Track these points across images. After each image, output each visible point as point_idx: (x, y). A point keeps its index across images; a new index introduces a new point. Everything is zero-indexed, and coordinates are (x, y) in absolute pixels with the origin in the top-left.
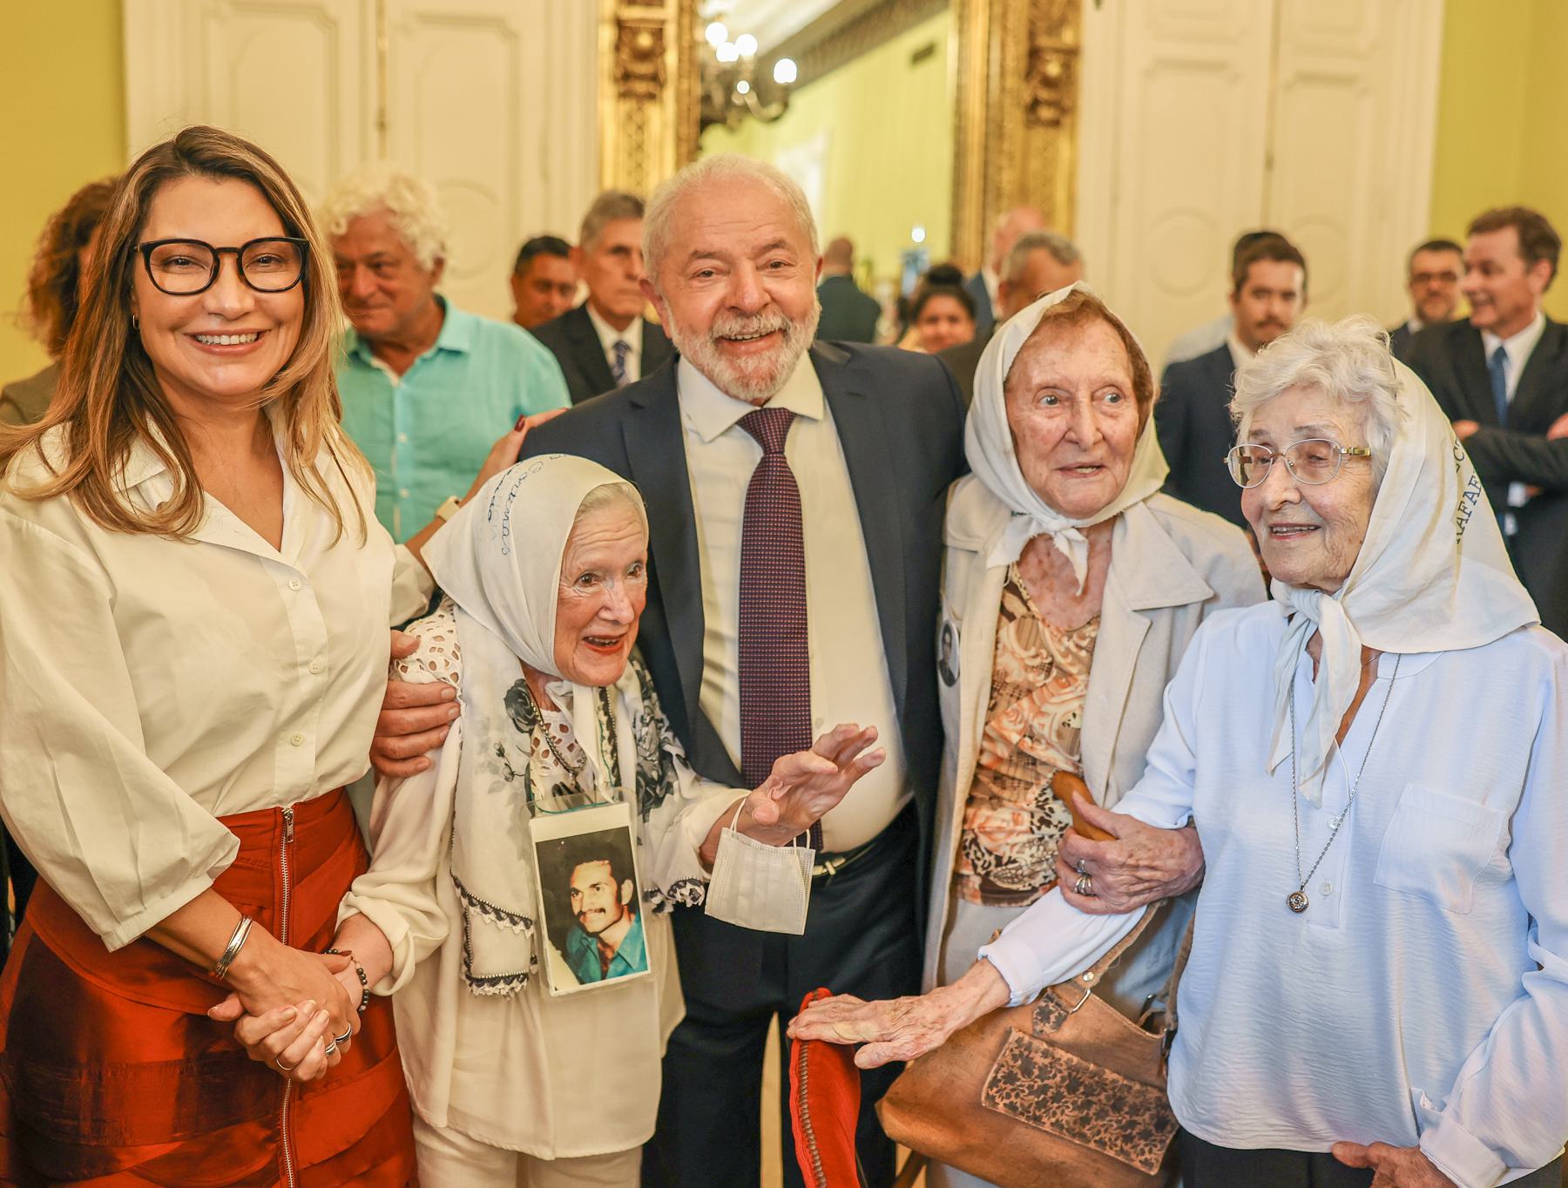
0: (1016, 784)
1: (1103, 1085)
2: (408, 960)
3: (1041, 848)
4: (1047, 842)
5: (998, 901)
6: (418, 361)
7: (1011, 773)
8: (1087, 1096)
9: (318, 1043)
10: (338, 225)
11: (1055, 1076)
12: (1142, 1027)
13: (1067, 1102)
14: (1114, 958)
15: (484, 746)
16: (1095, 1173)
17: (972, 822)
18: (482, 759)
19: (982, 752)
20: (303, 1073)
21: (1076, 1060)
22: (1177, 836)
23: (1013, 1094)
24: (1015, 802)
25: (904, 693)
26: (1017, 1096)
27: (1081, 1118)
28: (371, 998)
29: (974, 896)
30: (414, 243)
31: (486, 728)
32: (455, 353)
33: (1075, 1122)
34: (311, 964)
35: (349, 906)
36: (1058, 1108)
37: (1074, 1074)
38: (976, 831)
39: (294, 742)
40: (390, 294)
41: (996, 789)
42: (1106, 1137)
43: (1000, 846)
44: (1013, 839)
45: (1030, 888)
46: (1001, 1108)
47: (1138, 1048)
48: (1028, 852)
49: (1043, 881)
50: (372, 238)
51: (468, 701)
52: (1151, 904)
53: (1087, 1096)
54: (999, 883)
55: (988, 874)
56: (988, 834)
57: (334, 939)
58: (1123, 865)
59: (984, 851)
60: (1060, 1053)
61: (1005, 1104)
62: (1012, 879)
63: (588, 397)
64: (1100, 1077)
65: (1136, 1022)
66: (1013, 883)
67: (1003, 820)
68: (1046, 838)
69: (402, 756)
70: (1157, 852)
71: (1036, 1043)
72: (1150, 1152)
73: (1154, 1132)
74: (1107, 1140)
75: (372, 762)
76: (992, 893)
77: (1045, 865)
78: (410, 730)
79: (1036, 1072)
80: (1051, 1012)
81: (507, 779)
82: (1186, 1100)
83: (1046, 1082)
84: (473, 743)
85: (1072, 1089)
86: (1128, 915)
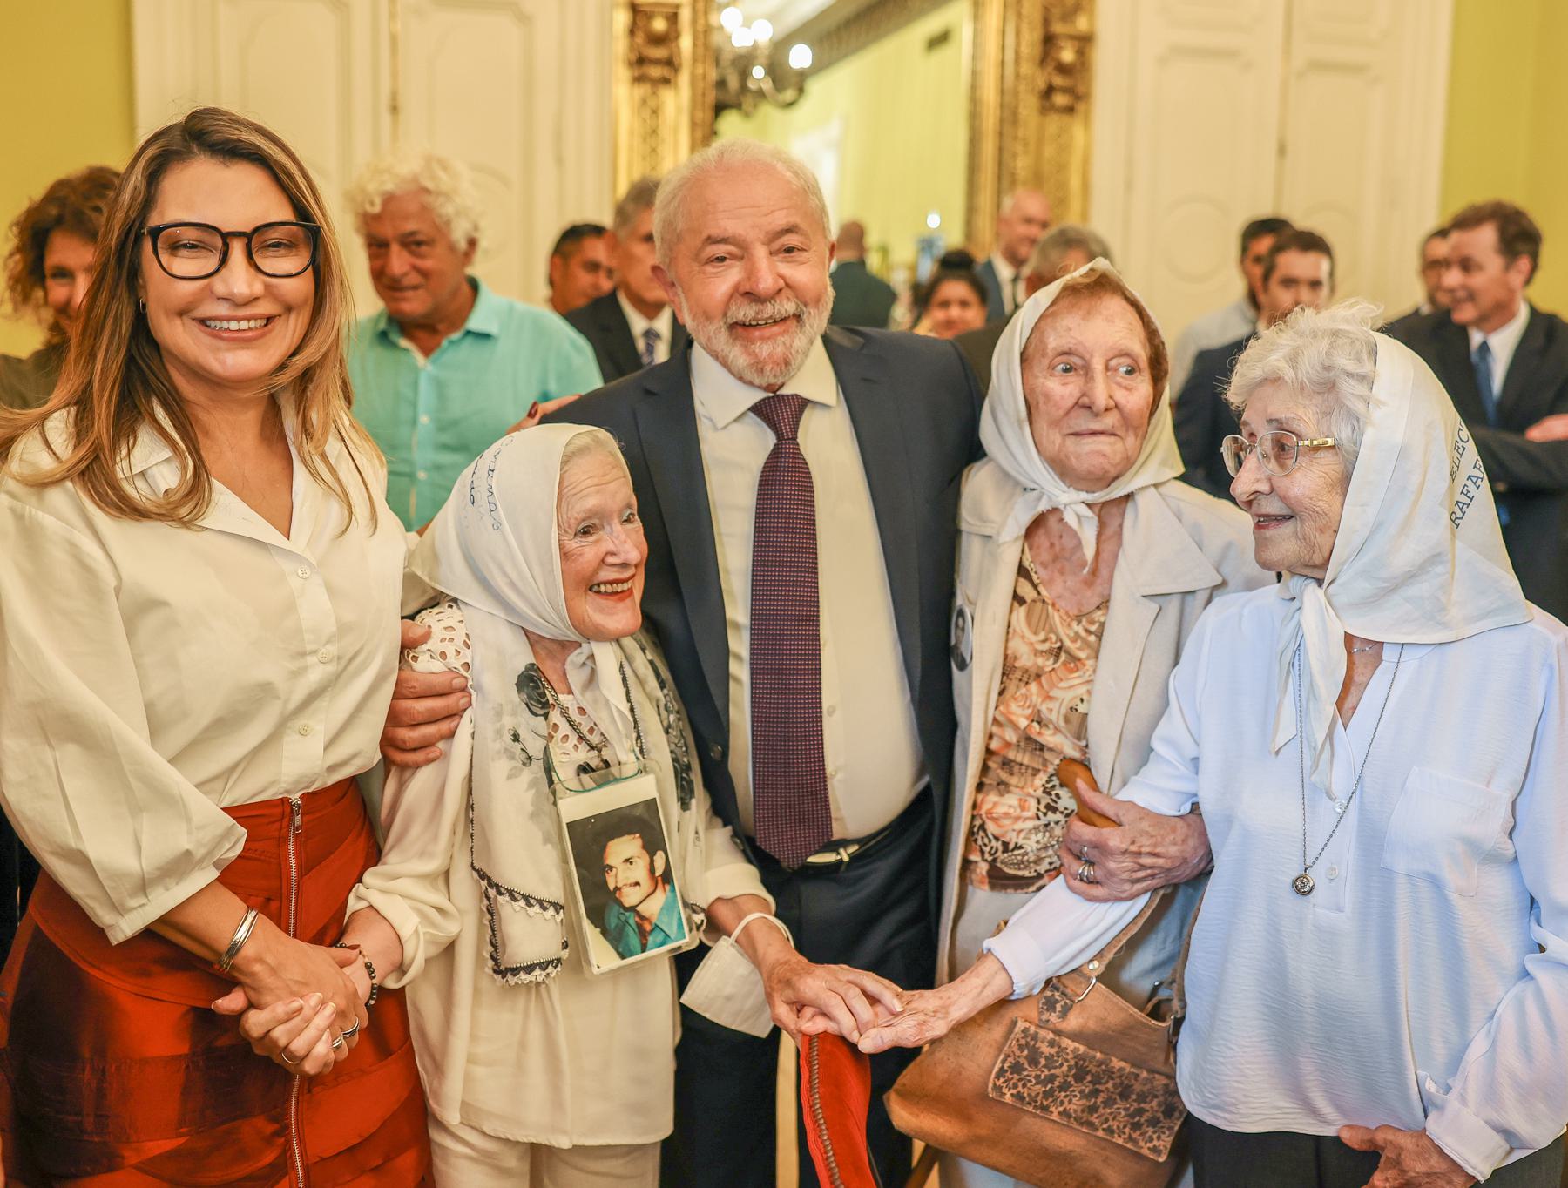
0: (1023, 771)
1: (1110, 1074)
2: (418, 953)
3: (1047, 834)
4: (1052, 828)
5: (1004, 887)
6: (445, 343)
7: (1019, 759)
8: (1094, 1085)
9: (324, 1037)
10: (372, 204)
11: (1062, 1065)
12: (1148, 1015)
13: (1074, 1091)
14: (1119, 946)
15: (499, 733)
16: (1104, 1161)
17: (980, 808)
18: (497, 746)
19: (991, 737)
21: (1082, 1049)
22: (1180, 823)
24: (1022, 788)
25: (918, 679)
26: (1024, 1086)
28: (380, 992)
29: (982, 883)
30: (448, 223)
31: (499, 714)
32: (484, 336)
33: (1083, 1111)
34: (320, 956)
35: (359, 898)
38: (984, 816)
39: (301, 731)
40: (425, 274)
41: (1004, 775)
42: (1114, 1124)
43: (1006, 832)
44: (1020, 825)
45: (1035, 874)
46: (1008, 1098)
47: (1145, 1036)
48: (1034, 838)
49: (1048, 867)
50: (406, 217)
51: (479, 688)
52: (1155, 891)
53: (1094, 1085)
54: (1006, 870)
55: (994, 860)
56: (995, 820)
57: (342, 933)
58: (1125, 852)
59: (991, 837)
60: (1066, 1042)
61: (1012, 1095)
62: (1020, 864)
63: (617, 378)
64: (1107, 1066)
65: (1141, 1010)
66: (1020, 869)
67: (1010, 806)
68: (1052, 824)
69: (413, 747)
70: (1159, 838)
71: (1042, 1033)
72: (1159, 1138)
73: (1162, 1119)
74: (1115, 1127)
75: (382, 752)
76: (999, 880)
77: (1050, 852)
78: (420, 719)
80: (1057, 1001)
81: (524, 764)
82: (1193, 1085)
83: (1053, 1071)
84: (488, 730)
85: (1079, 1078)
86: (1131, 902)
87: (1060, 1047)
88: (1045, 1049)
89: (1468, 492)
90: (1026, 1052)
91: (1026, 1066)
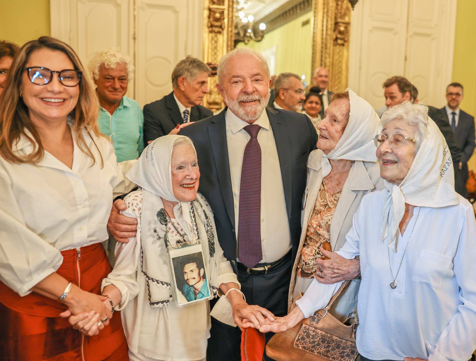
1: (333, 341)
8: (328, 344)
20: (90, 333)
23: (304, 343)
26: (305, 344)
27: (327, 351)
36: (319, 347)
37: (323, 337)
46: (300, 348)
53: (328, 344)
61: (302, 347)
83: (314, 340)
85: (323, 342)
91: (306, 338)
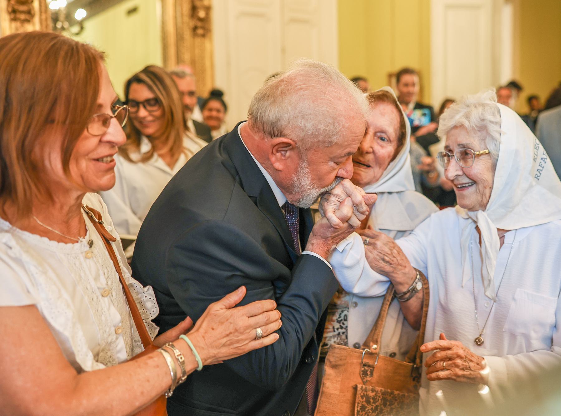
11: (378, 400)
79: (372, 401)
87: (376, 391)
88: (371, 394)
89: (542, 165)
90: (364, 399)
